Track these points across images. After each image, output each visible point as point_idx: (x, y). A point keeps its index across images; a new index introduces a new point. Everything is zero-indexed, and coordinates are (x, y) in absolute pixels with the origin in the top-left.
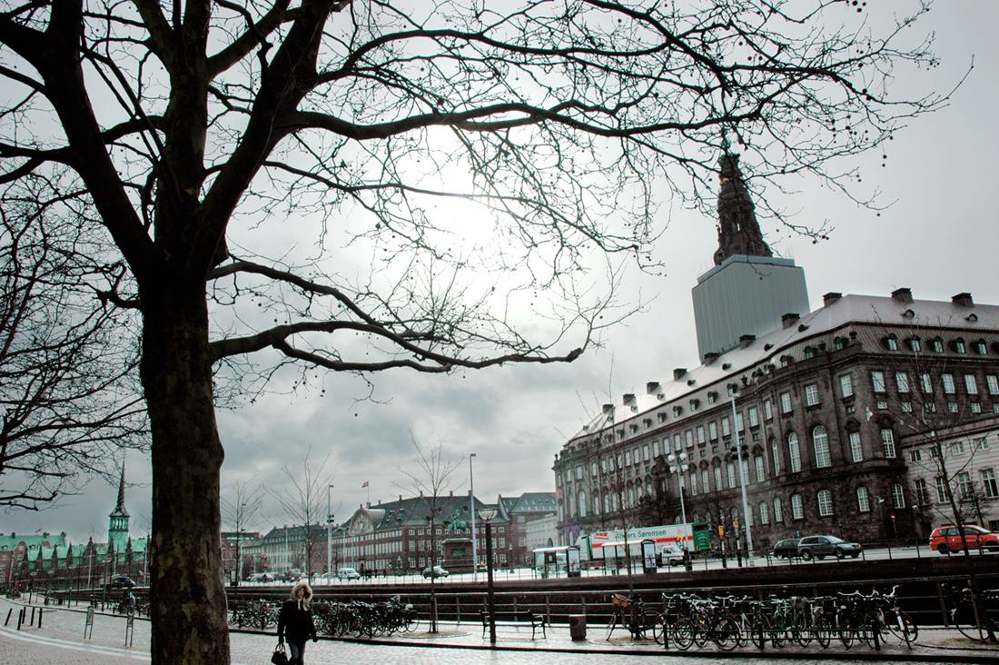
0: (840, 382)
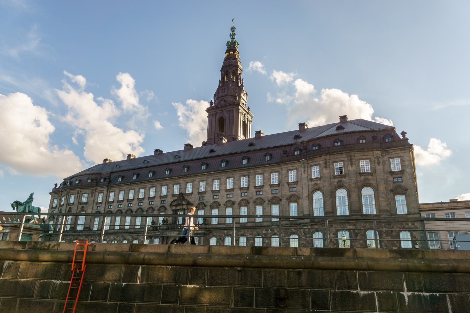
0: (389, 161)
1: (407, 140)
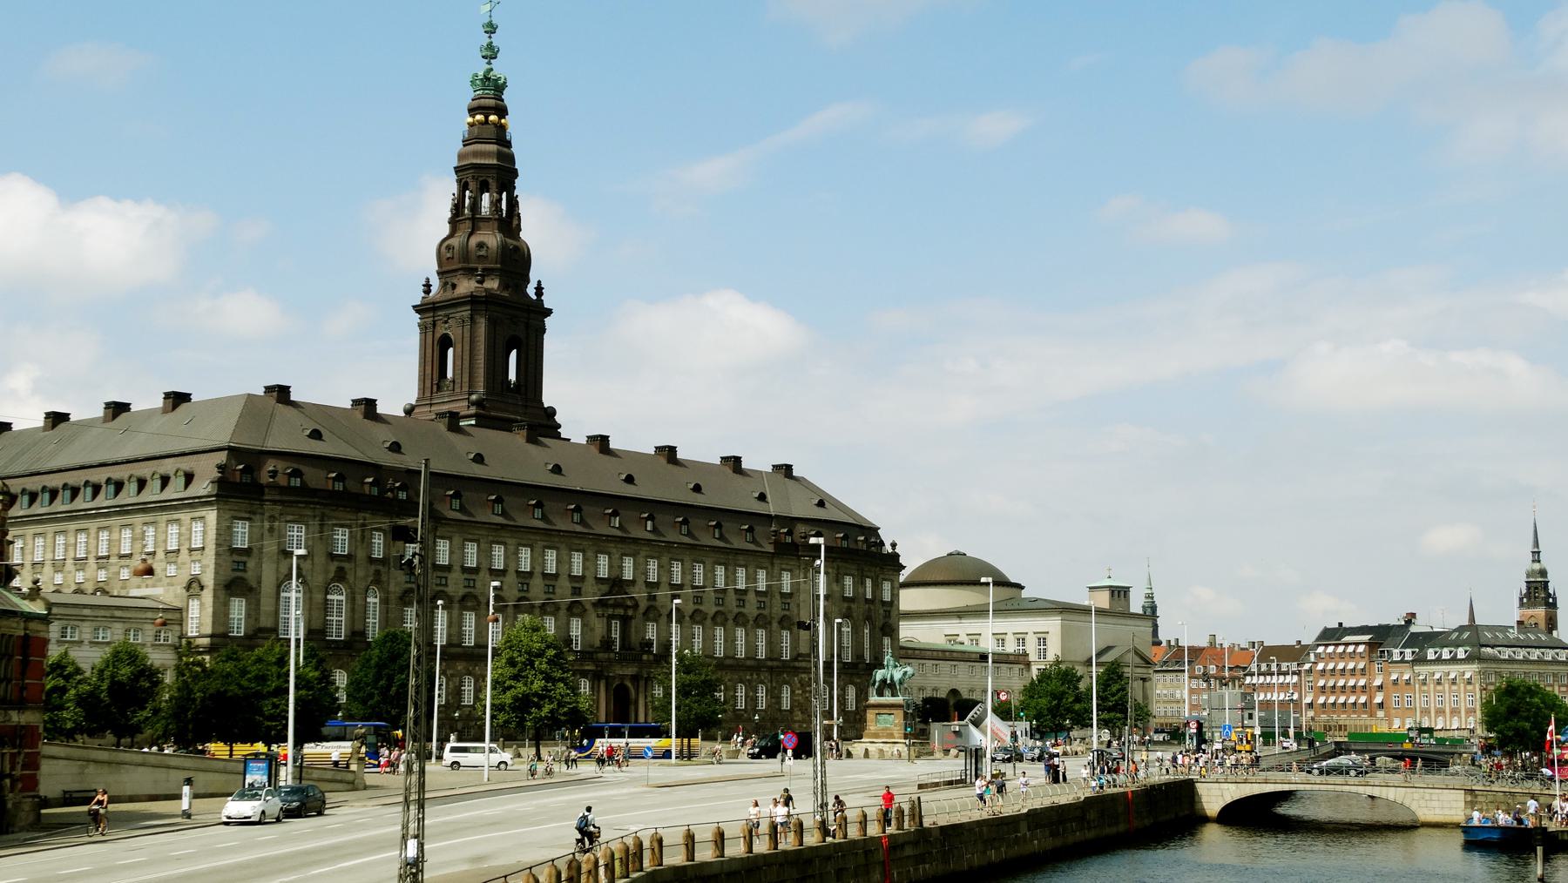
1: (898, 556)
